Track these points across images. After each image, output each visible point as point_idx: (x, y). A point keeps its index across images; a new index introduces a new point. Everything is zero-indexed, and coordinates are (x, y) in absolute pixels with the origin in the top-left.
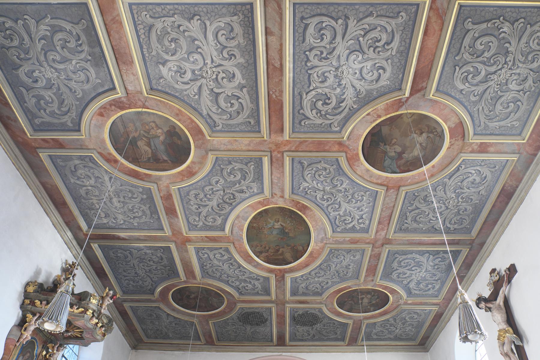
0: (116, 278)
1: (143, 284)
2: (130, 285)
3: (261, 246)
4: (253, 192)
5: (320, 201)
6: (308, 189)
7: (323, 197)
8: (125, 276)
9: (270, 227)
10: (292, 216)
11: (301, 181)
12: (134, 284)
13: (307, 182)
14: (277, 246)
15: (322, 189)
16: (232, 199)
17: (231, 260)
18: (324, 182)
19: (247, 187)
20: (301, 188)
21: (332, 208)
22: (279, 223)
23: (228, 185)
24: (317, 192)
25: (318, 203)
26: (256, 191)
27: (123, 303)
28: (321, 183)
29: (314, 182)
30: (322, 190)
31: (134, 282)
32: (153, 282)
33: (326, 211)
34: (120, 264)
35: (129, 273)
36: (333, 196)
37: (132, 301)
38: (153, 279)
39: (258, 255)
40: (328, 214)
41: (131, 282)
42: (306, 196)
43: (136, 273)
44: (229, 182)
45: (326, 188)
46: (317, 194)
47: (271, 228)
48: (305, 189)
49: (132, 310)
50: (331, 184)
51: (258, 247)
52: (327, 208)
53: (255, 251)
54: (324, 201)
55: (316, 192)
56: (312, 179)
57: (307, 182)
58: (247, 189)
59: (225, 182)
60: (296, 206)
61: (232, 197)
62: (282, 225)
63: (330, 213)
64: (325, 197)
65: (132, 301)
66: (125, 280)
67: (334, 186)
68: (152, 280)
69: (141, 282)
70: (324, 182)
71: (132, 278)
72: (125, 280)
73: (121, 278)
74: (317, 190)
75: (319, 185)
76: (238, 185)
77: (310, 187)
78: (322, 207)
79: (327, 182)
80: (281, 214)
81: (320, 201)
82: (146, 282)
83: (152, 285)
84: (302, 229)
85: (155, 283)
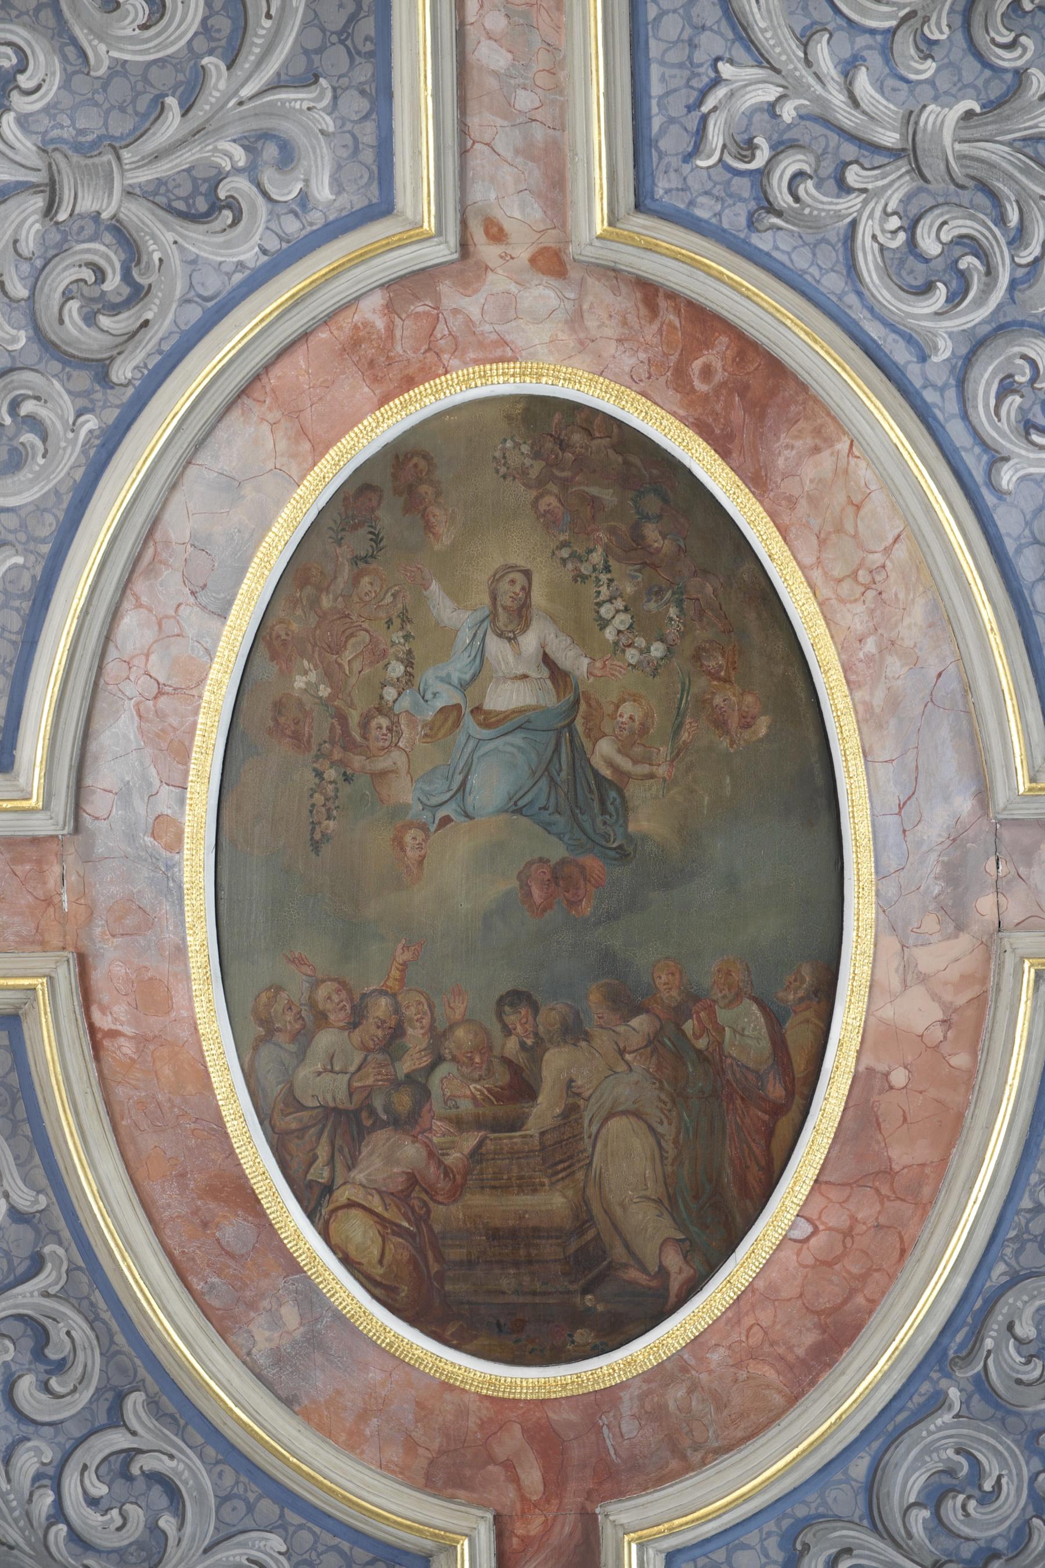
3: (356, 1018)
4: (304, 199)
5: (884, 295)
6: (781, 147)
7: (912, 242)
9: (448, 697)
10: (651, 533)
11: (712, 44)
13: (762, 60)
14: (516, 998)
15: (890, 138)
16: (115, 309)
17: (37, 1264)
18: (905, 46)
19: (251, 144)
20: (715, 136)
21: (1007, 388)
22: (530, 642)
23: (90, 122)
24: (853, 176)
25: (874, 330)
26: (323, 192)
28: (875, 59)
29: (822, 51)
30: (895, 154)
33: (957, 432)
36: (1001, 220)
39: (320, 1173)
40: (974, 463)
42: (762, 242)
44: (106, 83)
45: (930, 116)
46: (854, 201)
47: (452, 714)
48: (751, 147)
50: (970, 67)
51: (325, 1040)
52: (961, 383)
53: (293, 1103)
54: (926, 289)
55: (843, 188)
56: (801, 22)
57: (762, 60)
58: (251, 172)
59: (66, 84)
60: (680, 379)
61: (113, 282)
62: (557, 674)
63: (997, 459)
64: (929, 245)
67: (996, 90)
70: (905, 46)
74: (849, 151)
75: (863, 82)
76: (172, 125)
77: (788, 112)
78: (914, 373)
79: (927, 48)
80: (549, 502)
81: (884, 295)
84: (747, 724)
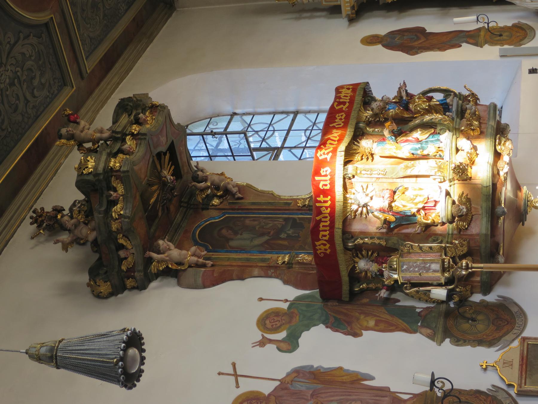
0: (37, 117)
1: (30, 56)
2: (43, 81)
8: (27, 101)
12: (38, 74)
27: (85, 75)
31: (33, 78)
32: (19, 39)
34: (4, 127)
35: (18, 98)
37: (76, 59)
38: (12, 42)
41: (36, 82)
43: (12, 84)
49: (95, 48)
65: (76, 59)
66: (35, 97)
68: (16, 43)
69: (29, 63)
71: (25, 87)
72: (35, 97)
73: (34, 107)
82: (23, 54)
83: (27, 37)
85: (20, 32)
